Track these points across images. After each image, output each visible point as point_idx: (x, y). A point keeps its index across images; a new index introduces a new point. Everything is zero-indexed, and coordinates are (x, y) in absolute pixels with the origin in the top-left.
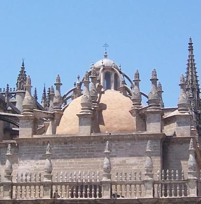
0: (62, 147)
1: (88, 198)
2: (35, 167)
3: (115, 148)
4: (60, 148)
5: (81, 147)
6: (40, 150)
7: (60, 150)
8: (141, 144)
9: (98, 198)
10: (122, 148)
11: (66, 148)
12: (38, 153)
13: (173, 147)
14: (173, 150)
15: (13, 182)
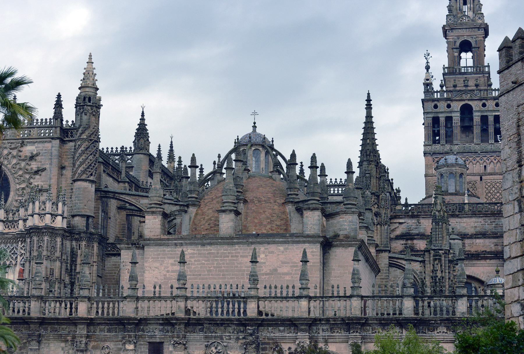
0: (198, 250)
1: (231, 317)
2: (165, 275)
3: (264, 253)
4: (195, 252)
5: (222, 251)
6: (171, 254)
7: (196, 254)
8: (297, 248)
9: (242, 315)
10: (272, 252)
11: (202, 252)
12: (169, 258)
13: (336, 251)
14: (336, 256)
15: (139, 295)
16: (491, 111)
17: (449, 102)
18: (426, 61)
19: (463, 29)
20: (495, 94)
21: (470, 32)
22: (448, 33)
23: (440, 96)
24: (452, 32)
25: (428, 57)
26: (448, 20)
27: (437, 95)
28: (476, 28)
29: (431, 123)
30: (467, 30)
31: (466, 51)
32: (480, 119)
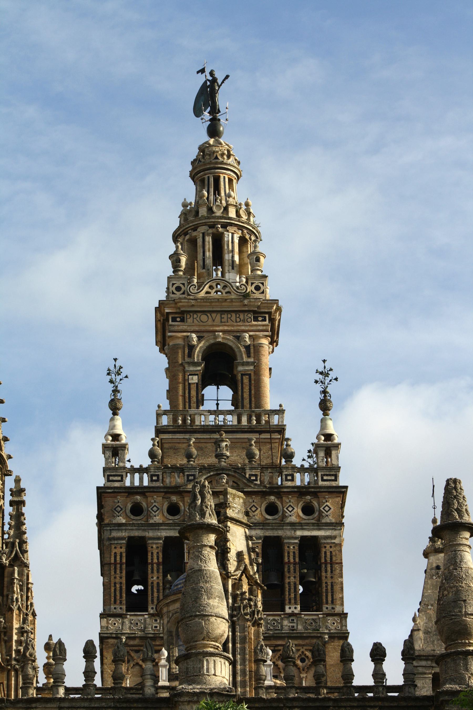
16: (293, 525)
17: (174, 498)
18: (110, 387)
19: (214, 315)
20: (302, 480)
21: (230, 323)
22: (170, 322)
23: (151, 480)
24: (182, 320)
25: (118, 378)
26: (173, 289)
27: (141, 479)
28: (249, 311)
29: (124, 555)
30: (225, 316)
31: (218, 384)
32: (260, 547)
